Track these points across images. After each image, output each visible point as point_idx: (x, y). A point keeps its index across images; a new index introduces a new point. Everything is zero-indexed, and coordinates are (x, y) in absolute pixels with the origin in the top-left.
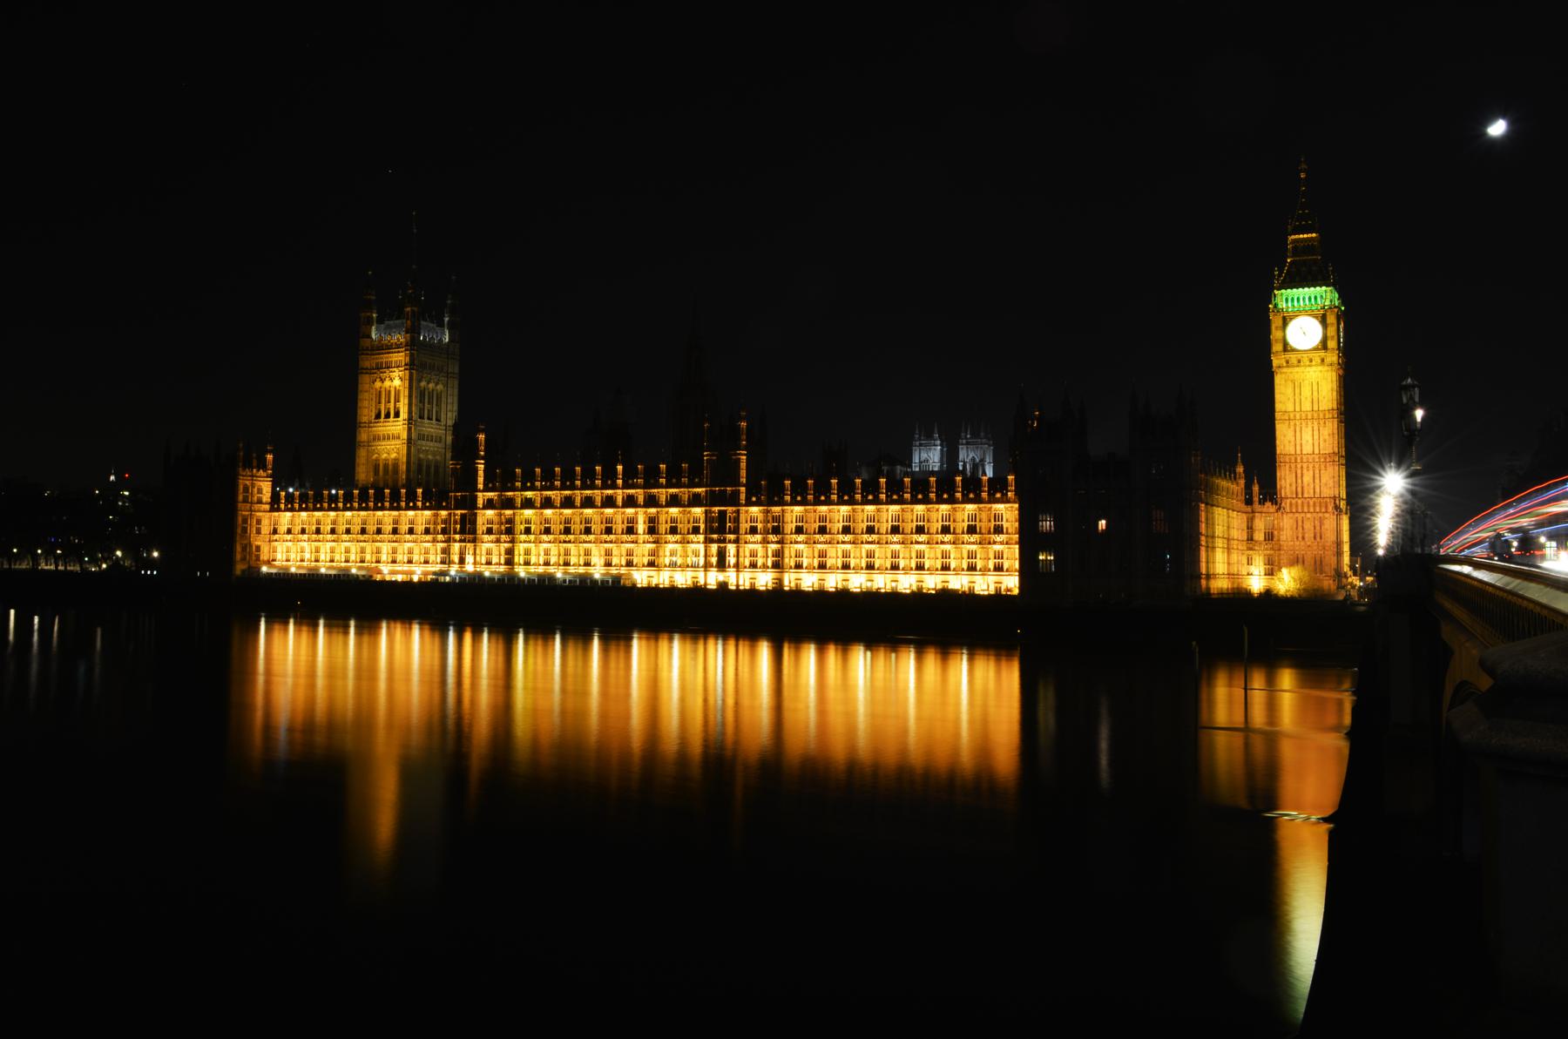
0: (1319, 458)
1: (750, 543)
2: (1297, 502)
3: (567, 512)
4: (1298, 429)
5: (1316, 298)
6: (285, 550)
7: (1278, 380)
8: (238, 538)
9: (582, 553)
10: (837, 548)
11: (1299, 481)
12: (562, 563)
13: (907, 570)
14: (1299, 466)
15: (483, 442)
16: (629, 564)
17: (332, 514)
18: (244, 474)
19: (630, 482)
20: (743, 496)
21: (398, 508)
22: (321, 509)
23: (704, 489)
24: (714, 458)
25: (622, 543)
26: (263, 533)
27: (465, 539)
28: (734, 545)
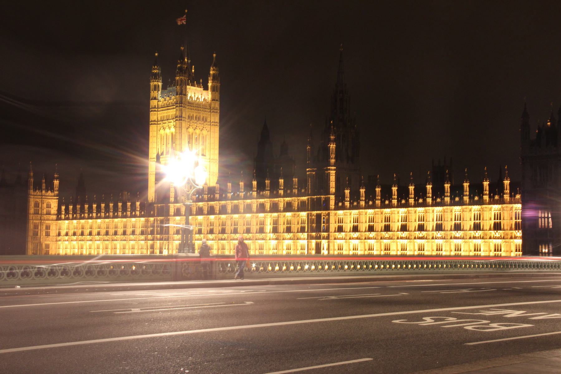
1: (338, 239)
8: (30, 239)
10: (397, 242)
17: (90, 221)
18: (35, 194)
19: (261, 193)
20: (332, 203)
24: (314, 173)
25: (256, 239)
26: (51, 234)
27: (163, 238)
28: (327, 241)
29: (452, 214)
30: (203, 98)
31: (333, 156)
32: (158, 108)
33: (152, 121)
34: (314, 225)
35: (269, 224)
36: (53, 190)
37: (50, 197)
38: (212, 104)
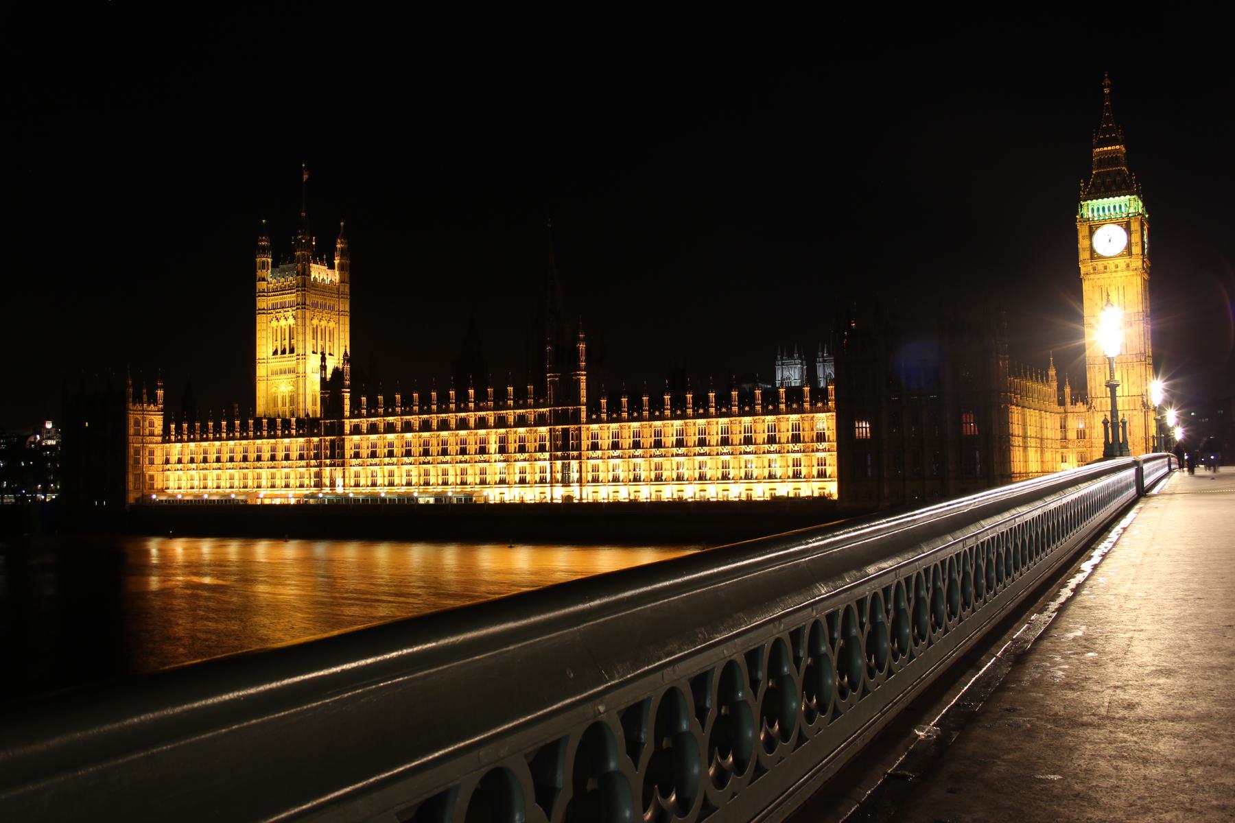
3: (426, 435)
7: (1086, 286)
8: (130, 469)
9: (440, 473)
16: (483, 482)
17: (217, 443)
18: (135, 408)
20: (584, 415)
21: (275, 437)
22: (207, 440)
23: (548, 409)
24: (557, 379)
25: (476, 462)
26: (155, 462)
27: (335, 463)
28: (577, 461)
29: (741, 426)
30: (329, 279)
31: (583, 358)
32: (267, 292)
33: (259, 310)
34: (559, 443)
35: (493, 442)
36: (157, 402)
37: (153, 413)
38: (341, 287)
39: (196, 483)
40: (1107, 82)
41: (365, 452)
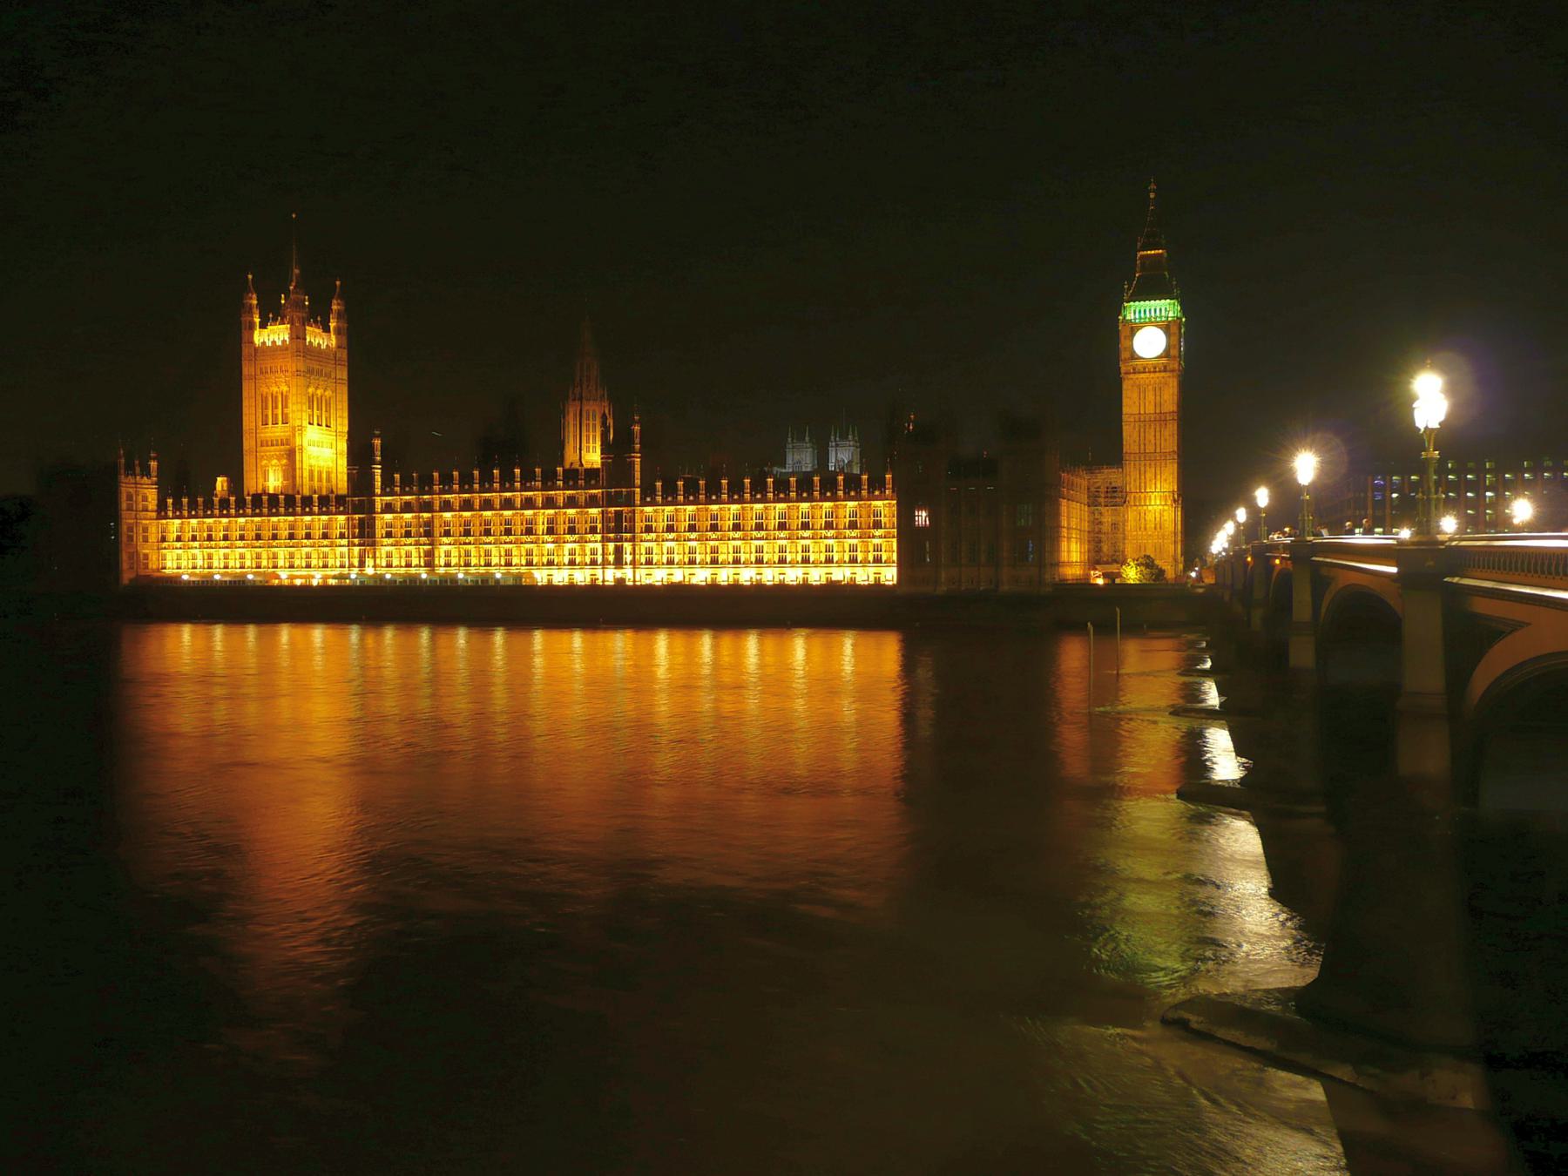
0: (1161, 456)
2: (1140, 496)
3: (467, 514)
4: (1142, 430)
5: (1161, 310)
6: (175, 558)
7: (1125, 385)
9: (482, 554)
11: (1143, 477)
12: (462, 564)
13: (793, 563)
14: (1143, 463)
15: (379, 448)
16: (530, 564)
17: (225, 520)
18: (127, 481)
20: (638, 497)
21: (294, 514)
23: (600, 491)
25: (522, 543)
28: (631, 543)
30: (325, 344)
31: (637, 440)
39: (199, 563)
40: (1153, 187)
41: (397, 531)
